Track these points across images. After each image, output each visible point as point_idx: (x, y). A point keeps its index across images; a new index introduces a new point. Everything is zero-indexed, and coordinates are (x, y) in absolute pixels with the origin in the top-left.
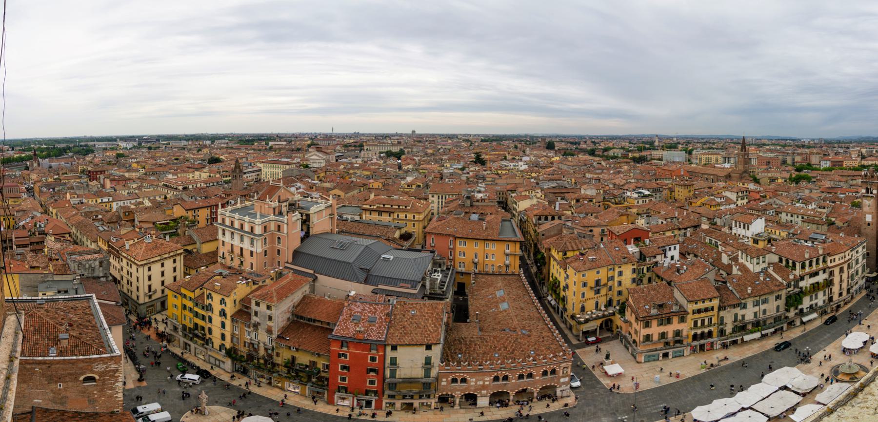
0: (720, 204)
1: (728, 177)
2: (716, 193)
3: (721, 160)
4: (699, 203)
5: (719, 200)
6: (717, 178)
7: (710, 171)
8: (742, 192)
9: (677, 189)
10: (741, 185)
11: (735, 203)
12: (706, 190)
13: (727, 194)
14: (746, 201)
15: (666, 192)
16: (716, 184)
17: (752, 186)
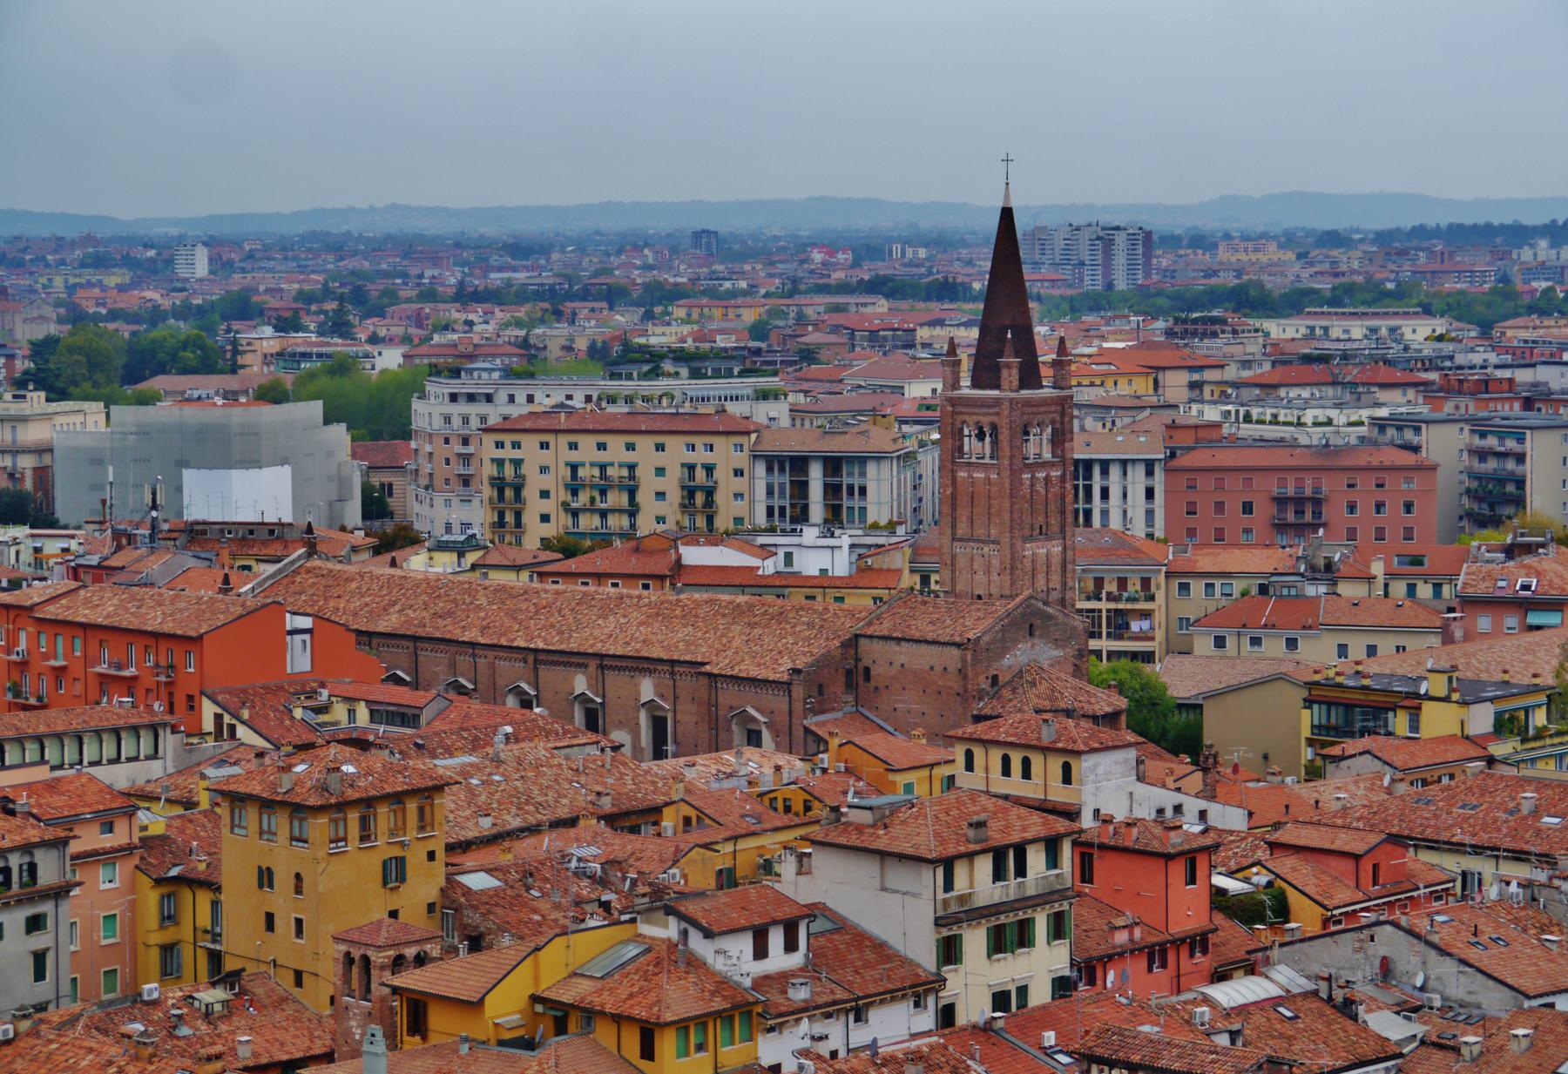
0: (750, 1011)
1: (848, 676)
2: (697, 872)
3: (746, 494)
4: (505, 1008)
5: (734, 958)
6: (707, 708)
7: (620, 622)
8: (1009, 859)
9: (238, 851)
10: (987, 775)
11: (920, 989)
12: (587, 849)
13: (838, 885)
14: (1041, 964)
15: (103, 902)
16: (701, 771)
17: (1112, 788)
